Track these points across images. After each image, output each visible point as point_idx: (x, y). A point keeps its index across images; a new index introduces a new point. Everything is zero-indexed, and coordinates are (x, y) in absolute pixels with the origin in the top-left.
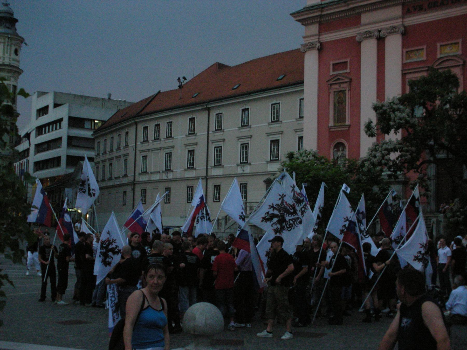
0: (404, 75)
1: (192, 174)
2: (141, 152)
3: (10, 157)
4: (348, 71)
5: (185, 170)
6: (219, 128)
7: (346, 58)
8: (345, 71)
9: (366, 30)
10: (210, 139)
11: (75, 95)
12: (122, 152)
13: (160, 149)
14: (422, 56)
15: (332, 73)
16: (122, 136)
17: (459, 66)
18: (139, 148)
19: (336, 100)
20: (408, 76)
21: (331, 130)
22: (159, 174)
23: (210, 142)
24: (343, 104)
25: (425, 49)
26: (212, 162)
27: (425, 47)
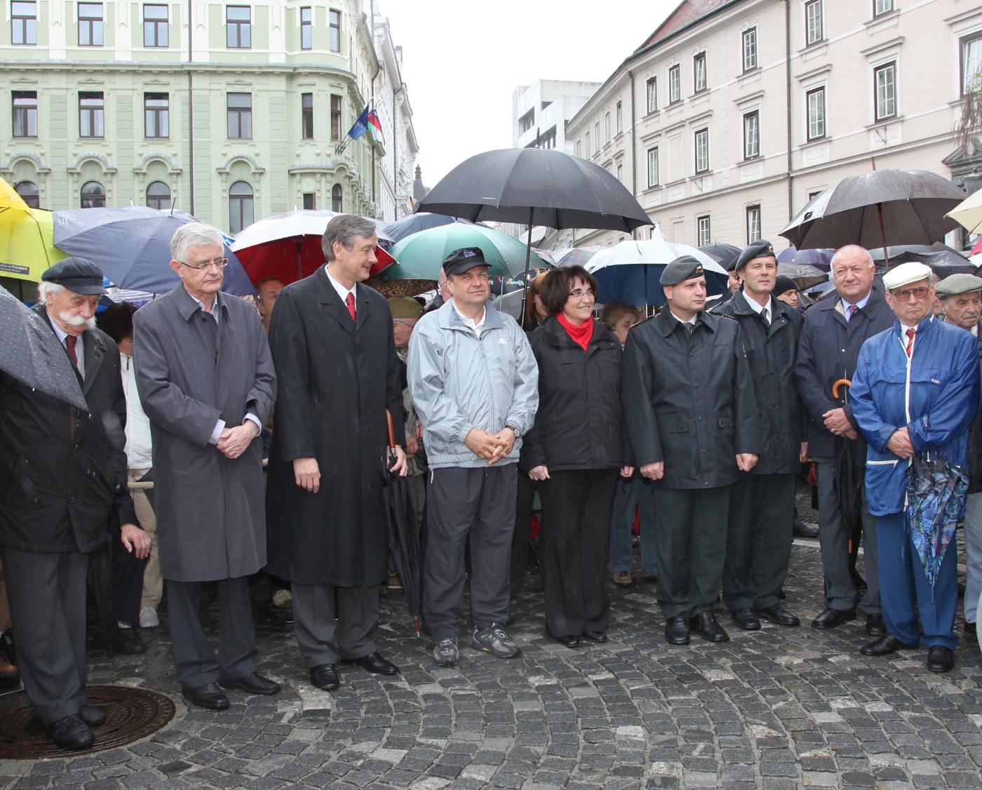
1: (755, 173)
2: (646, 139)
3: (335, 172)
5: (740, 165)
6: (816, 41)
10: (794, 73)
11: (581, 83)
12: (614, 150)
13: (681, 125)
16: (611, 115)
18: (642, 131)
22: (683, 185)
23: (794, 81)
26: (800, 137)
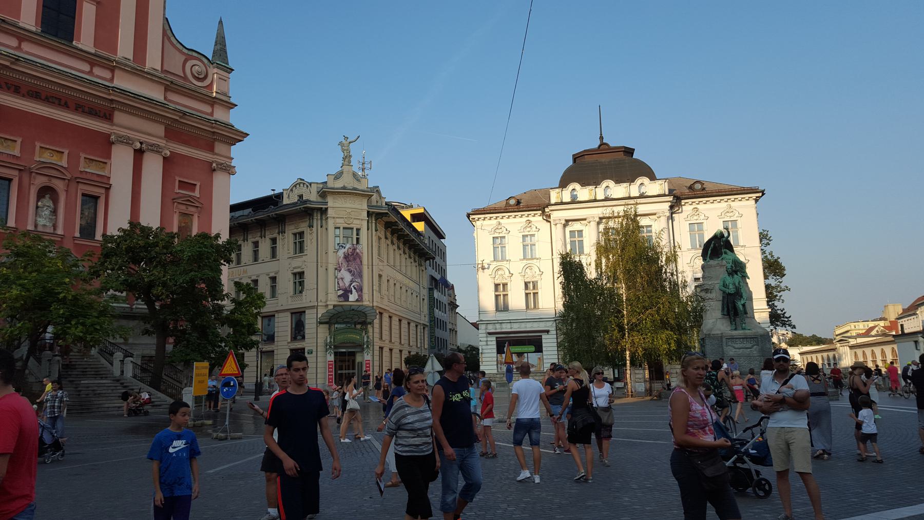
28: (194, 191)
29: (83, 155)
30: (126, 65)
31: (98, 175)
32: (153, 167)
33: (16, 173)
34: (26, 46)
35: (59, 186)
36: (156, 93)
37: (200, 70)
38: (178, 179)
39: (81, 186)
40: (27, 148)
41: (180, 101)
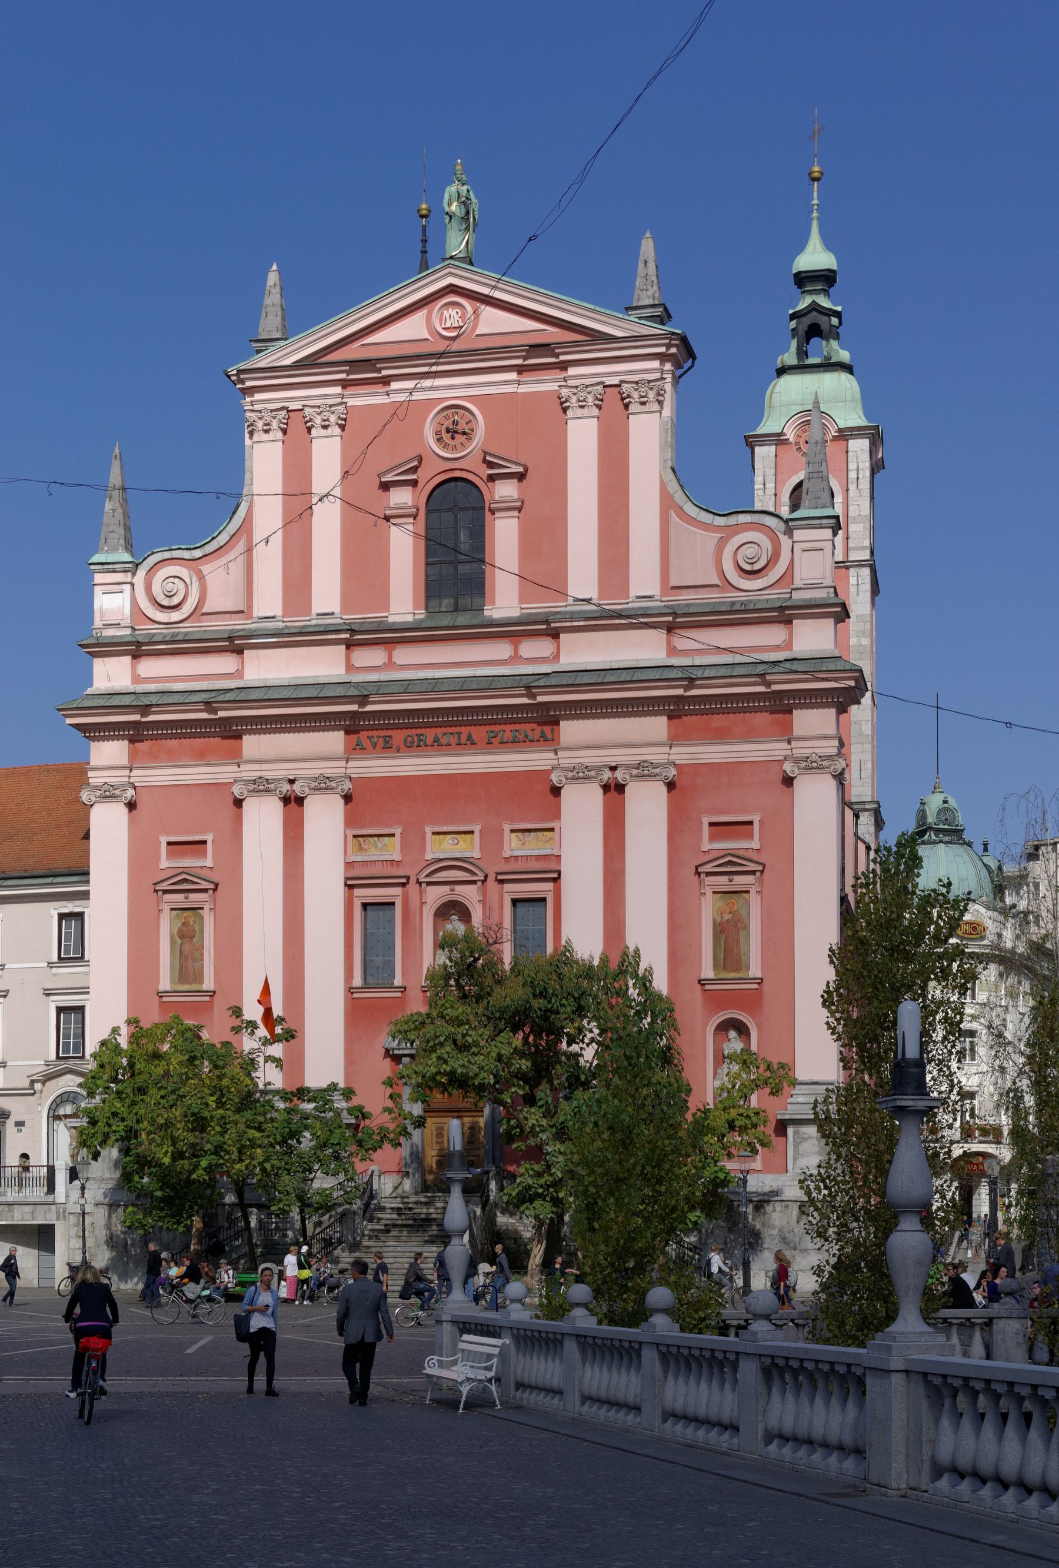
0: (350, 887)
4: (209, 862)
7: (204, 832)
8: (200, 863)
9: (259, 774)
14: (391, 850)
15: (164, 863)
17: (474, 882)
19: (175, 931)
20: (357, 892)
21: (165, 999)
24: (195, 940)
25: (397, 839)
27: (398, 831)
28: (751, 836)
29: (507, 827)
30: (573, 616)
31: (538, 857)
32: (647, 808)
33: (398, 891)
34: (404, 655)
35: (469, 895)
36: (645, 649)
37: (750, 551)
38: (706, 820)
39: (507, 887)
40: (413, 842)
41: (706, 647)
